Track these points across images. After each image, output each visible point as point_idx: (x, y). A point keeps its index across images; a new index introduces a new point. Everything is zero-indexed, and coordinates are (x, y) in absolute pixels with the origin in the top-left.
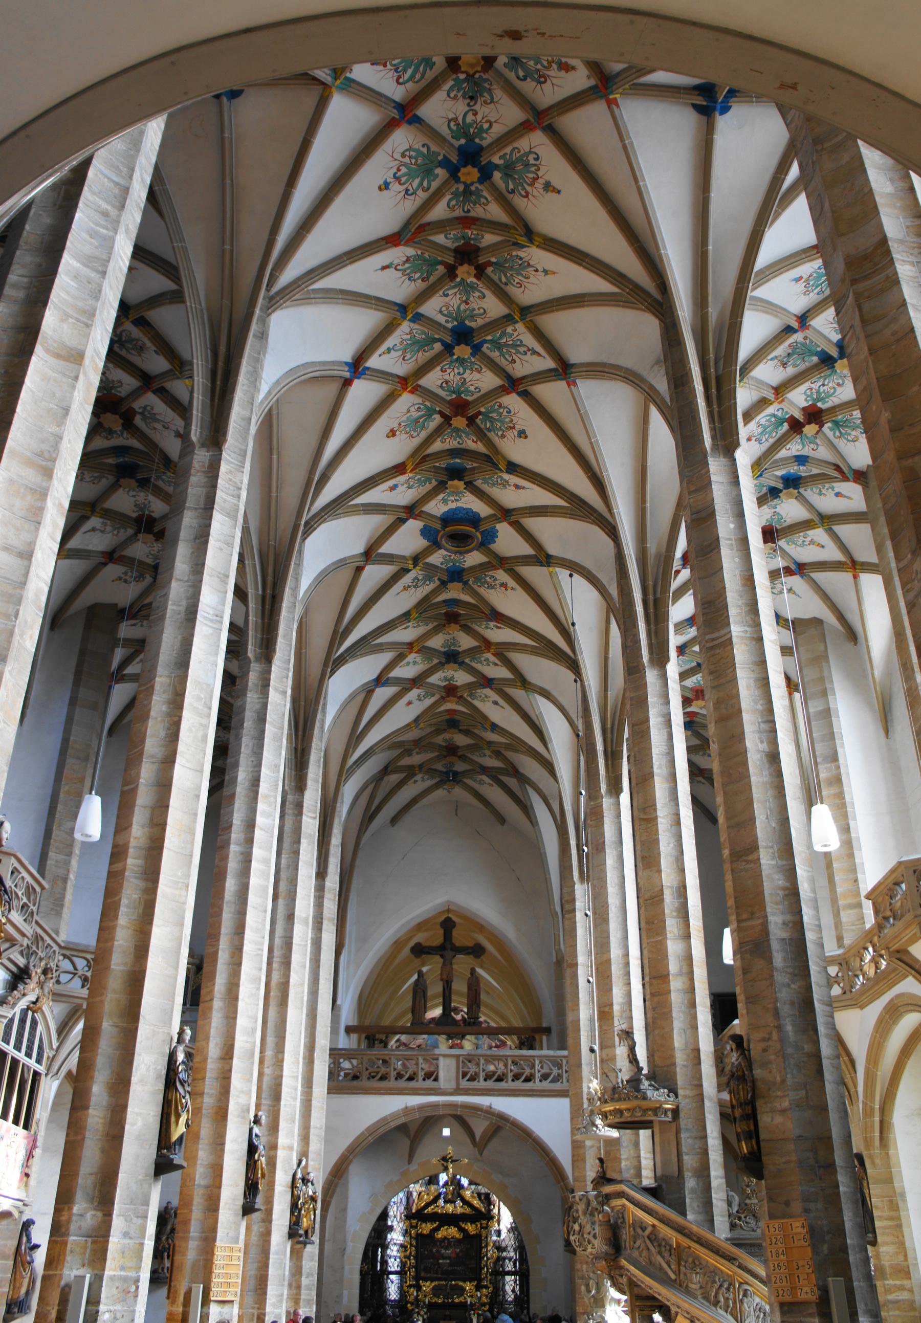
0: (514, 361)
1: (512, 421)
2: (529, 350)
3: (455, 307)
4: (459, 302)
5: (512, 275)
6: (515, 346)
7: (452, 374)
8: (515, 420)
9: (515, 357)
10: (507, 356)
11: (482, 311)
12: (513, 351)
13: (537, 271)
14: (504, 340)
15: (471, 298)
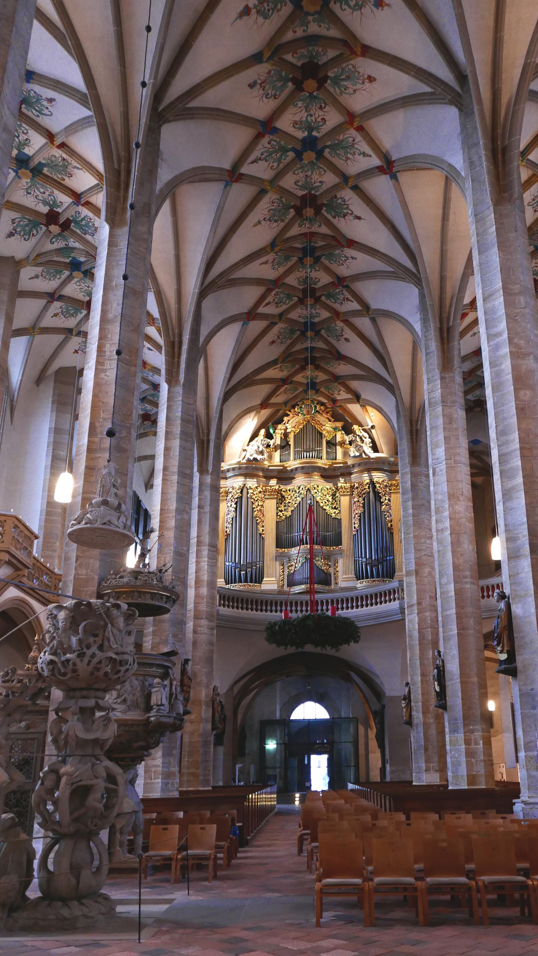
0: (269, 143)
1: (263, 90)
2: (260, 159)
3: (314, 173)
4: (312, 177)
5: (279, 206)
6: (270, 154)
7: (317, 116)
8: (261, 92)
9: (269, 146)
10: (275, 143)
11: (296, 173)
12: (271, 150)
13: (264, 219)
14: (278, 155)
15: (304, 179)
